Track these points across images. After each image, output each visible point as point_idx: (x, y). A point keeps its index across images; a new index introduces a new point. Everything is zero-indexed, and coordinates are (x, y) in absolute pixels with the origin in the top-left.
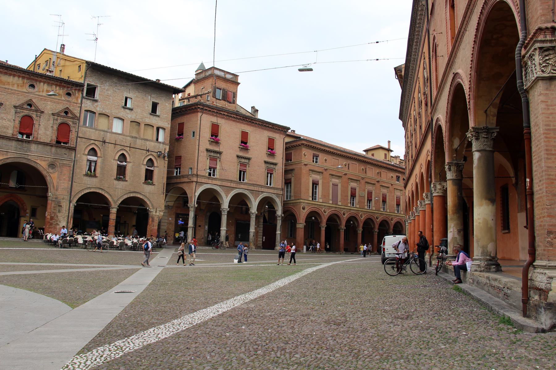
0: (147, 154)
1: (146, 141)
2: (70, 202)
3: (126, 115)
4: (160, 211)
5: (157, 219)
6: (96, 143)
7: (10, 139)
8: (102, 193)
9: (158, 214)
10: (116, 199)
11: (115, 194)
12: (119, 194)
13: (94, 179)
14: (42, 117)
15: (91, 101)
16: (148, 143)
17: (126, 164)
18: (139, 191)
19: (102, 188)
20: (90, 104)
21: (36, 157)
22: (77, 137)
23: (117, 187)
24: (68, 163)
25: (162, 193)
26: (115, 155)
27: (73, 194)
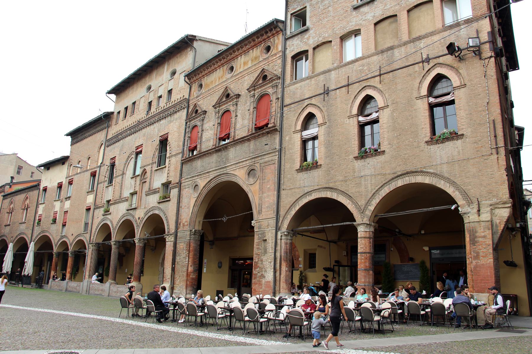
0: (426, 69)
1: (417, 43)
2: (277, 229)
3: (364, 17)
4: (494, 207)
5: (488, 233)
6: (313, 101)
7: (210, 153)
8: (333, 198)
9: (485, 216)
10: (362, 203)
11: (359, 192)
12: (370, 188)
13: (315, 173)
14: (239, 103)
15: (299, 36)
16: (422, 44)
17: (377, 114)
18: (418, 166)
19: (331, 185)
20: (298, 42)
21: (234, 166)
22: (283, 106)
23: (362, 174)
24: (270, 159)
25: (494, 151)
26: (351, 107)
27: (282, 213)
